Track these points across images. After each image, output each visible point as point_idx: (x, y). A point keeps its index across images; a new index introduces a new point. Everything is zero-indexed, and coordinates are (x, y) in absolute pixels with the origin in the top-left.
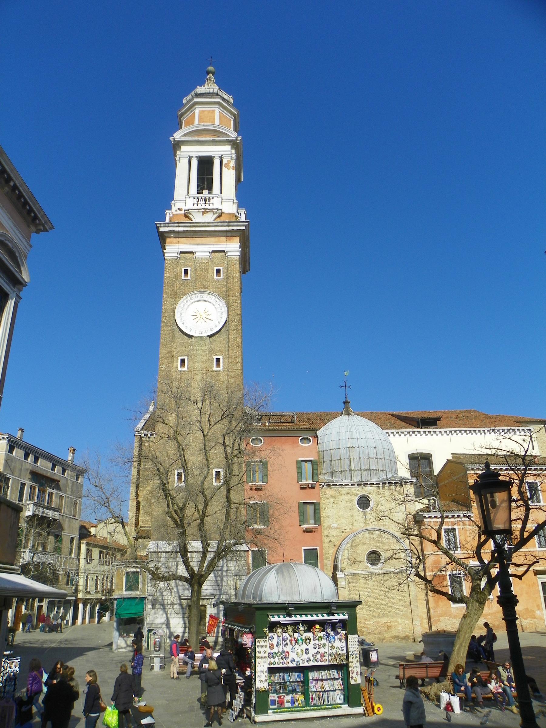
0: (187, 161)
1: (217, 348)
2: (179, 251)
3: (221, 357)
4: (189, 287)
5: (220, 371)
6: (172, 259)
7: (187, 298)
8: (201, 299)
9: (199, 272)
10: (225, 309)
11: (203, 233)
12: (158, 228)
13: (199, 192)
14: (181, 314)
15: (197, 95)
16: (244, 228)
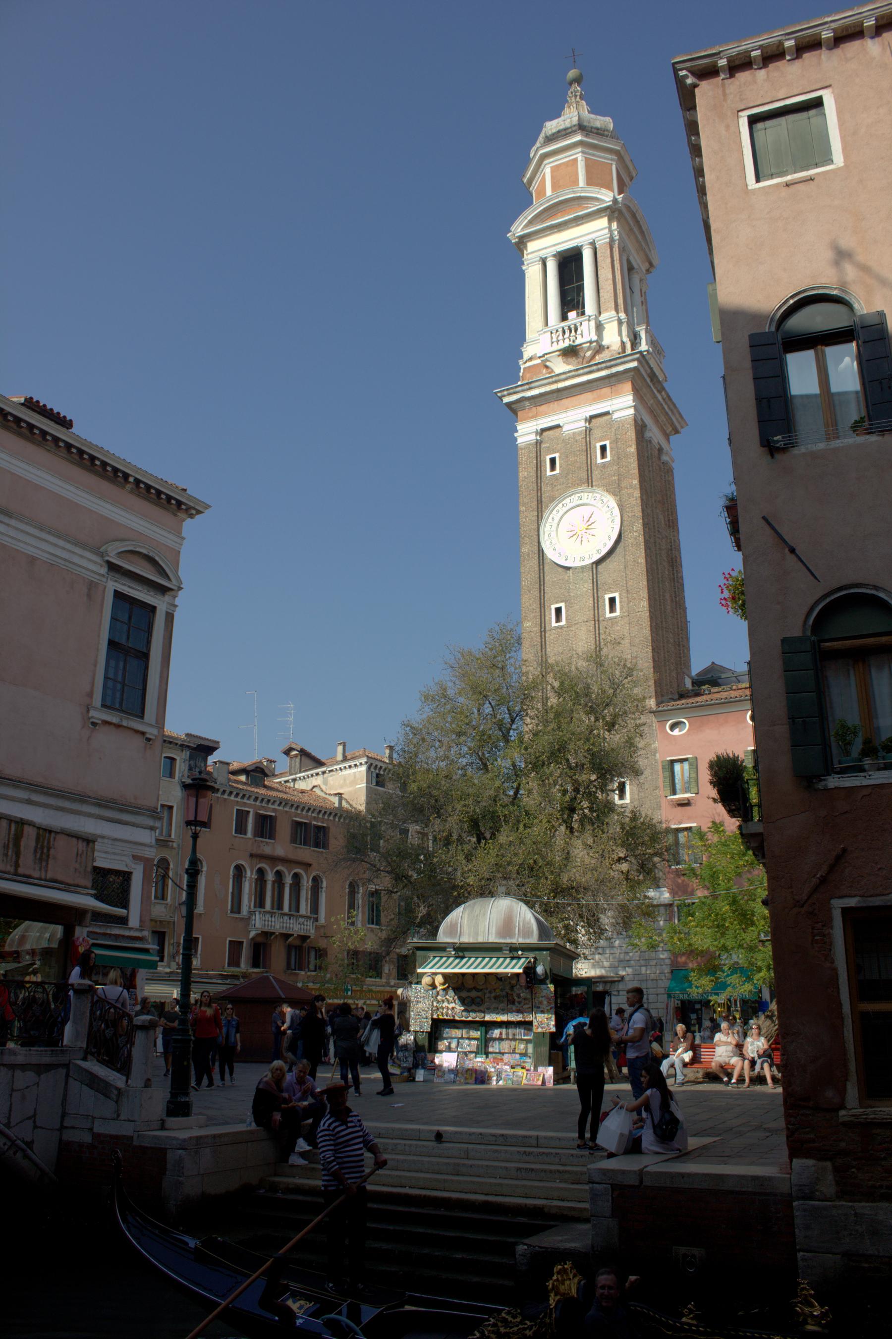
0: (538, 267)
1: (610, 581)
2: (539, 427)
3: (616, 595)
4: (559, 487)
5: (616, 618)
6: (528, 446)
7: (556, 506)
8: (580, 502)
9: (572, 459)
10: (617, 511)
11: (572, 390)
12: (501, 398)
13: (564, 318)
14: (549, 535)
15: (550, 139)
16: (634, 364)
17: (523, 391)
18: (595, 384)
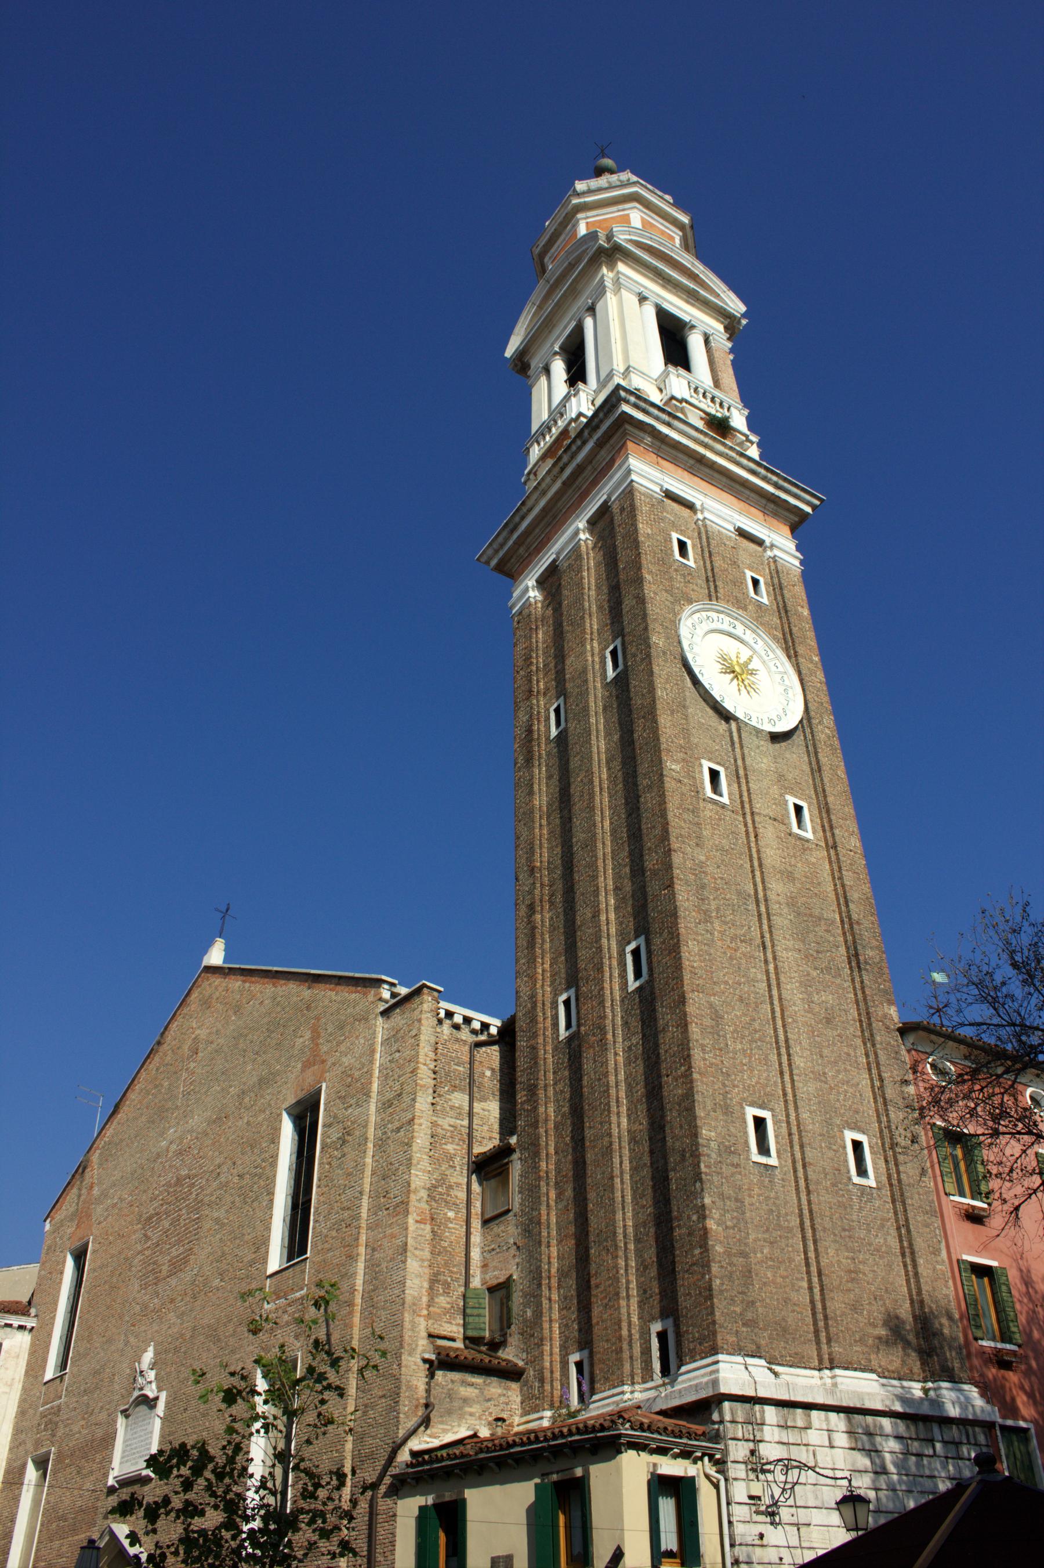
17: (657, 418)
18: (748, 492)
